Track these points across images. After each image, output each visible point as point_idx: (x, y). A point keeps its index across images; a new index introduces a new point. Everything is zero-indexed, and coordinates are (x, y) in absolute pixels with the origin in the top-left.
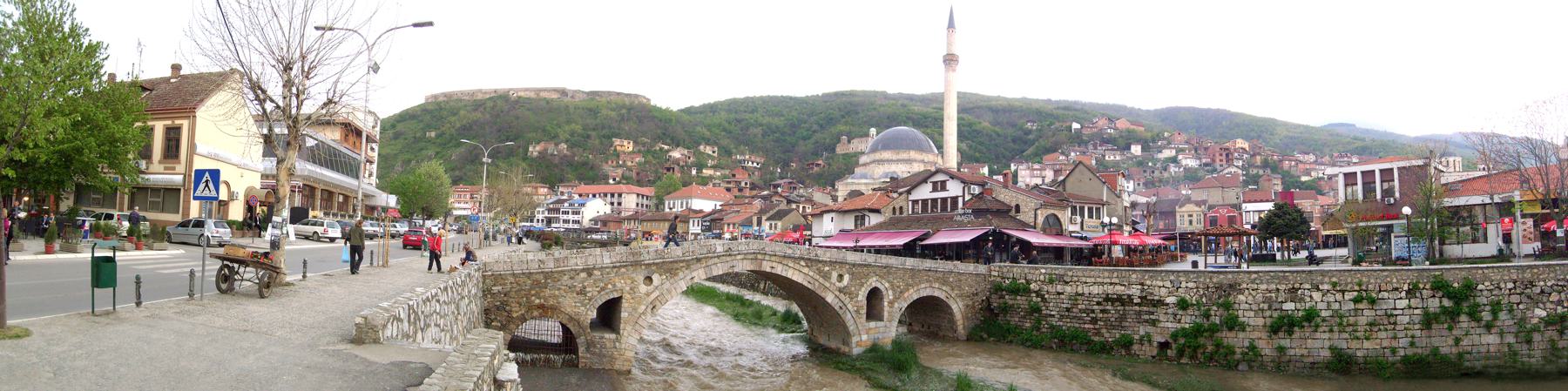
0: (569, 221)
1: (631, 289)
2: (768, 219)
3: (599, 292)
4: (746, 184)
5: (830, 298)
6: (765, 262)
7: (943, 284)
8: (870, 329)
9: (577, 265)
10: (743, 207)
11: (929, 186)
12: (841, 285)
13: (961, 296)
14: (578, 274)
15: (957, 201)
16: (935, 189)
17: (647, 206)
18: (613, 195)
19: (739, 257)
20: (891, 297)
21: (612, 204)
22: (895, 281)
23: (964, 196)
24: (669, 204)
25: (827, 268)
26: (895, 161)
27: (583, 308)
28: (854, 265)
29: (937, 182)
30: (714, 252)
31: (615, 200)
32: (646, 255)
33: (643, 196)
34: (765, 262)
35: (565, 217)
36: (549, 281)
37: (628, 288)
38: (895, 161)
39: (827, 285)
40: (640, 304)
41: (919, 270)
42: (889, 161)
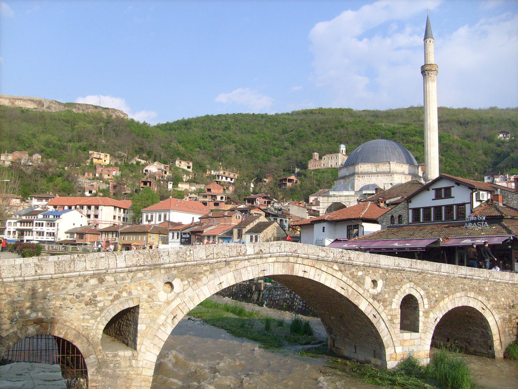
0: (43, 232)
1: (149, 297)
2: (249, 232)
3: (112, 301)
4: (222, 198)
5: (363, 306)
6: (297, 266)
7: (479, 294)
8: (405, 340)
9: (86, 270)
11: (432, 194)
13: (498, 307)
14: (87, 281)
15: (465, 209)
16: (438, 197)
18: (89, 207)
19: (271, 260)
20: (426, 306)
21: (89, 216)
22: (431, 289)
23: (471, 203)
24: (147, 217)
25: (360, 273)
26: (374, 173)
27: (92, 321)
28: (387, 270)
29: (440, 189)
30: (244, 255)
31: (92, 212)
32: (166, 258)
33: (120, 208)
34: (297, 266)
35: (39, 229)
36: (48, 289)
37: (145, 296)
38: (374, 173)
39: (361, 291)
40: (159, 313)
41: (454, 278)
42: (370, 174)
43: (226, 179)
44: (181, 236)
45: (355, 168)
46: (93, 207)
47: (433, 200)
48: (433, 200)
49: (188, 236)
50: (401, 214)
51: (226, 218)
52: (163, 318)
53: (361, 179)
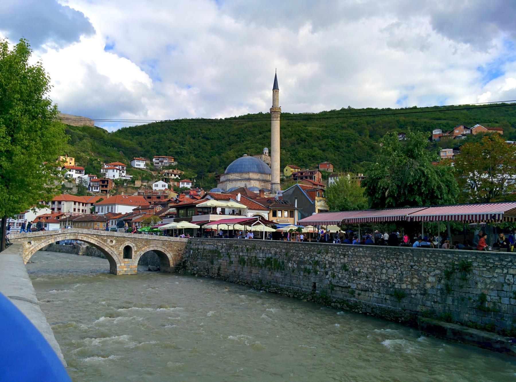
6: (78, 236)
10: (148, 211)
12: (112, 244)
17: (83, 210)
18: (53, 203)
19: (68, 234)
25: (105, 238)
28: (118, 237)
31: (56, 206)
33: (79, 203)
34: (78, 236)
39: (106, 244)
43: (175, 176)
46: (56, 203)
52: (27, 253)
53: (231, 183)
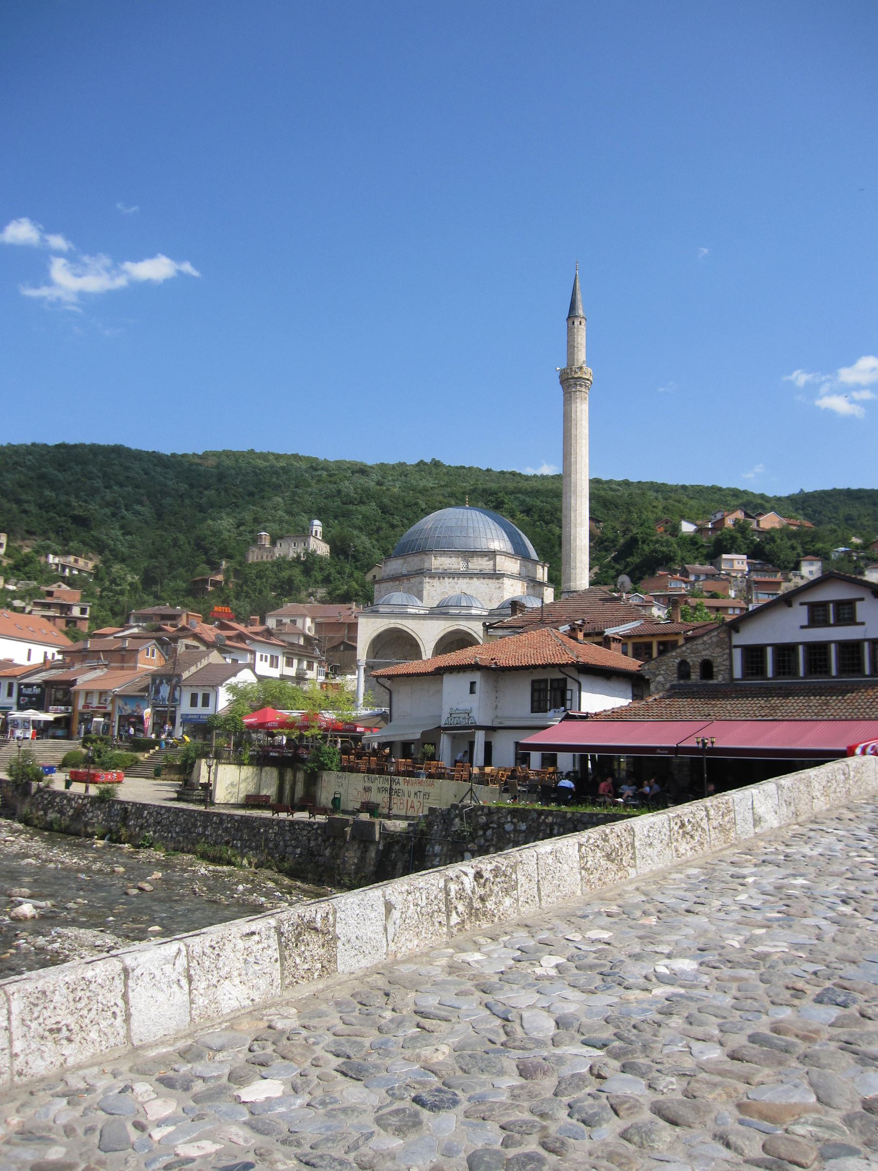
11: (799, 614)
29: (824, 605)
44: (20, 690)
45: (423, 561)
47: (802, 627)
48: (802, 627)
49: (37, 691)
50: (710, 658)
51: (124, 653)
53: (436, 582)
